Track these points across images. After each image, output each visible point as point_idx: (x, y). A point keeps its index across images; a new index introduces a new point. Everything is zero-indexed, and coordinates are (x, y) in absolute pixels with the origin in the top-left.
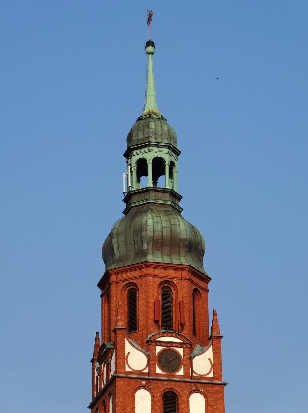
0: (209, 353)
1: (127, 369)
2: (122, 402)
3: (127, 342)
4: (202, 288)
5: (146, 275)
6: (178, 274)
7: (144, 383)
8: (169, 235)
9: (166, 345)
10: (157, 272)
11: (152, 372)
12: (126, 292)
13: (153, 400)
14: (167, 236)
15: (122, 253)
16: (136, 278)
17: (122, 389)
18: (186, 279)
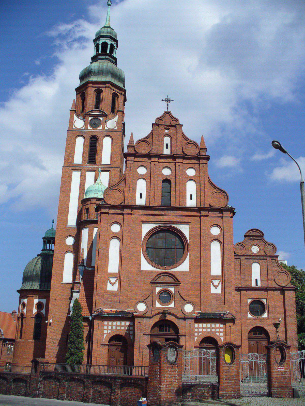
1: (74, 128)
3: (75, 115)
6: (104, 86)
11: (86, 128)
18: (107, 87)
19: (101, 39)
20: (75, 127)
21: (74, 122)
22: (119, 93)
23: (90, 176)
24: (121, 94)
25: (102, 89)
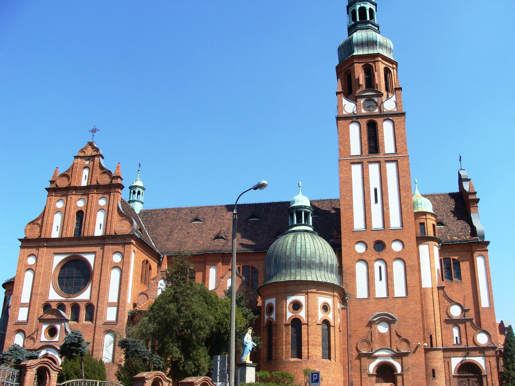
0: (394, 98)
1: (344, 113)
2: (341, 131)
4: (391, 67)
8: (366, 40)
9: (367, 97)
12: (346, 75)
14: (365, 41)
15: (343, 57)
16: (349, 66)
19: (357, 3)
21: (344, 107)
22: (391, 67)
23: (374, 169)
24: (393, 68)
25: (371, 64)
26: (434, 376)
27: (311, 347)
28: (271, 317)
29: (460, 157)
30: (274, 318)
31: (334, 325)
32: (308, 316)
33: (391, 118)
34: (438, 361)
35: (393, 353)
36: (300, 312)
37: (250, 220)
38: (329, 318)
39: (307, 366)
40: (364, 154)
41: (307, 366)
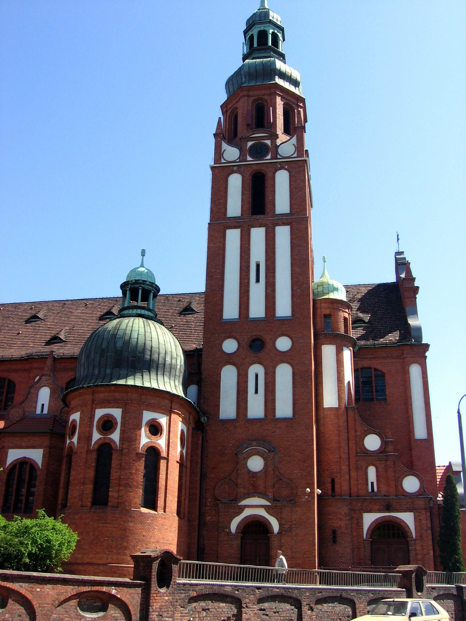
1: (223, 161)
3: (223, 142)
4: (295, 104)
5: (242, 97)
6: (269, 92)
7: (235, 168)
10: (251, 93)
13: (243, 180)
16: (236, 103)
17: (217, 175)
20: (225, 160)
21: (223, 153)
22: (295, 104)
25: (266, 97)
26: (335, 542)
27: (124, 488)
28: (72, 440)
29: (398, 235)
30: (76, 443)
31: (166, 456)
32: (122, 439)
33: (286, 167)
34: (342, 517)
35: (268, 503)
36: (112, 433)
37: (104, 317)
38: (159, 445)
39: (114, 519)
40: (245, 216)
41: (114, 519)
